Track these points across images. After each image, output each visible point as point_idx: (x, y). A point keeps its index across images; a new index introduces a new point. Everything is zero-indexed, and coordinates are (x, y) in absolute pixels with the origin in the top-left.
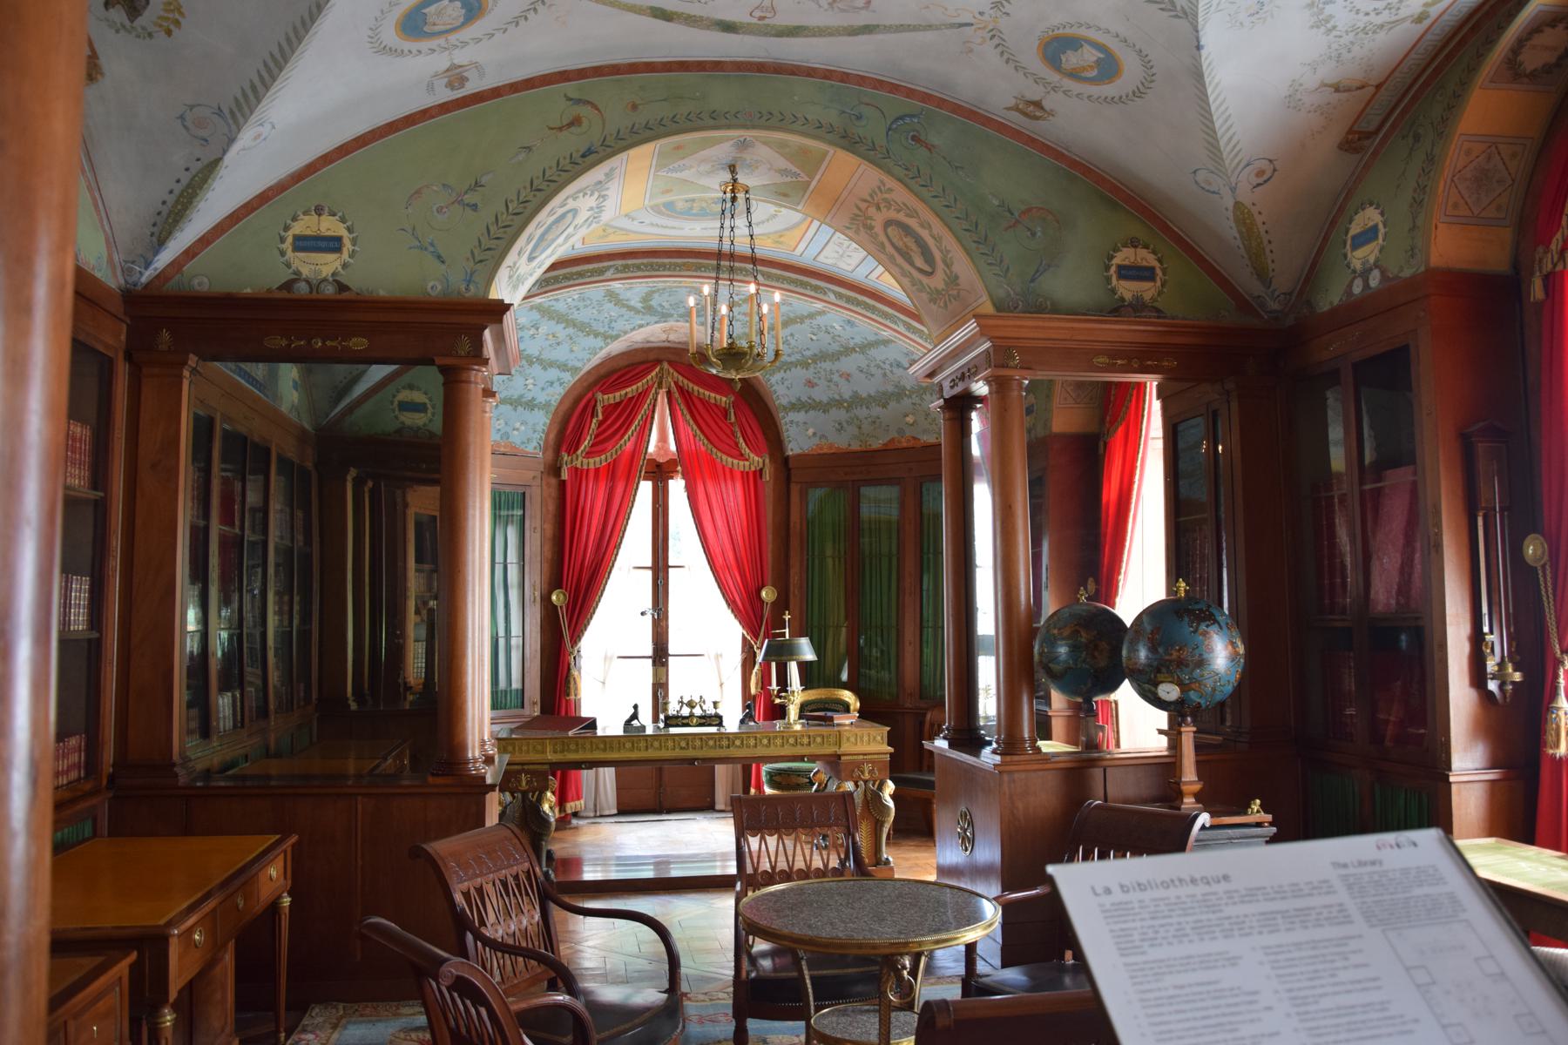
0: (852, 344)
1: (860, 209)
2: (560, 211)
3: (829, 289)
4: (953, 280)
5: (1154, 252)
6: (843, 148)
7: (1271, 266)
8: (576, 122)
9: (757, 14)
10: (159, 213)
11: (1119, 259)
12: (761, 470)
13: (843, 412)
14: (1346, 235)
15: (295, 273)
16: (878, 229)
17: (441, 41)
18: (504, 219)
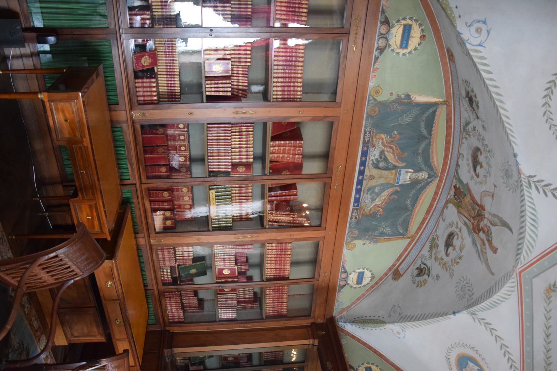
10: (362, 317)
15: (357, 369)
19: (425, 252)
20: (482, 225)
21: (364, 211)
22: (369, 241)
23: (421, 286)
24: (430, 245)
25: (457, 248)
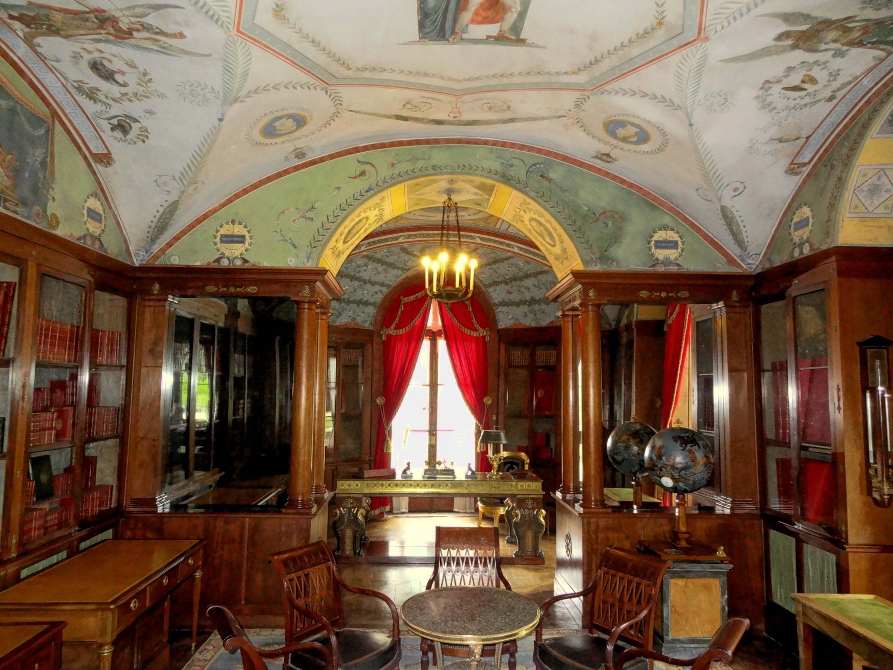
0: (529, 272)
2: (357, 220)
4: (564, 250)
5: (678, 233)
6: (502, 182)
8: (363, 173)
9: (452, 115)
13: (526, 307)
17: (287, 137)
18: (327, 225)
19: (91, 107)
20: (124, 27)
21: (7, 188)
22: (51, 190)
23: (147, 137)
24: (85, 96)
25: (125, 68)
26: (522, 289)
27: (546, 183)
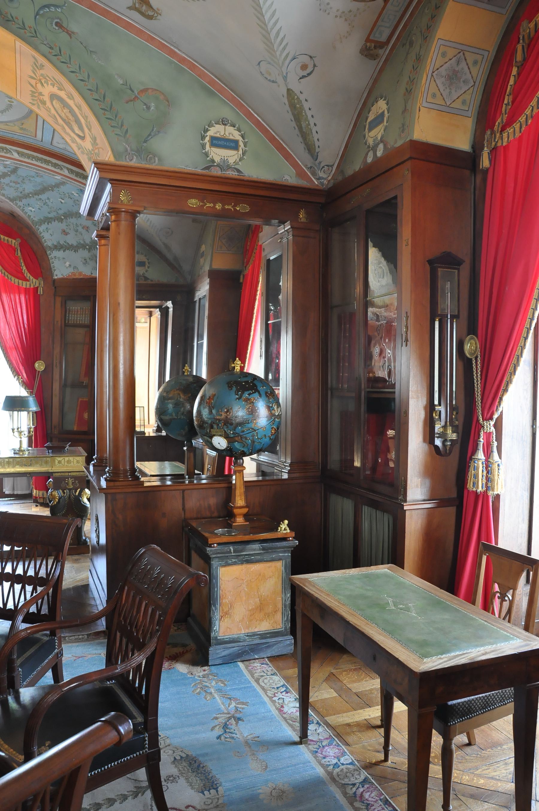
1: (32, 86)
3: (65, 167)
5: (239, 130)
7: (317, 144)
11: (212, 132)
12: (37, 288)
13: (86, 252)
14: (366, 122)
16: (48, 104)
26: (80, 229)
27: (64, 35)
